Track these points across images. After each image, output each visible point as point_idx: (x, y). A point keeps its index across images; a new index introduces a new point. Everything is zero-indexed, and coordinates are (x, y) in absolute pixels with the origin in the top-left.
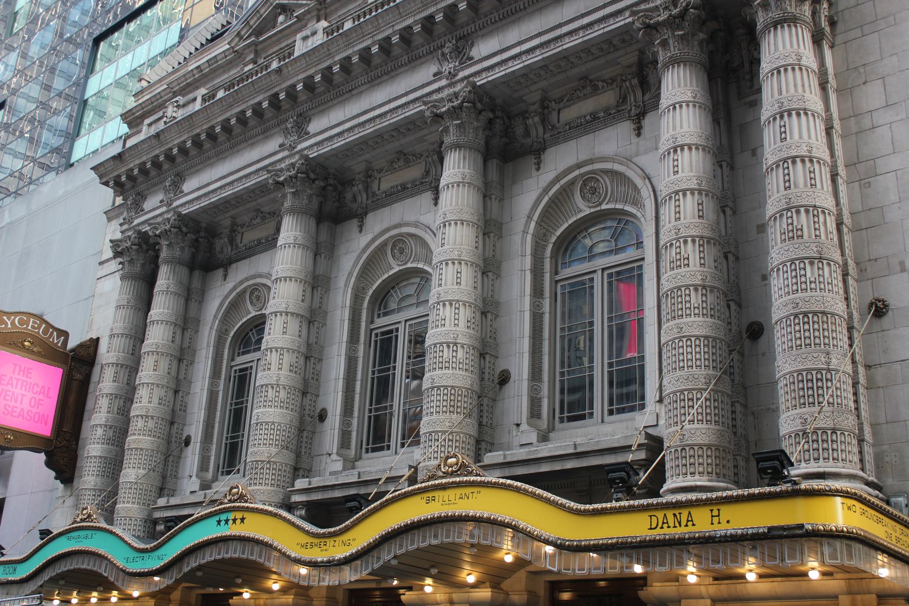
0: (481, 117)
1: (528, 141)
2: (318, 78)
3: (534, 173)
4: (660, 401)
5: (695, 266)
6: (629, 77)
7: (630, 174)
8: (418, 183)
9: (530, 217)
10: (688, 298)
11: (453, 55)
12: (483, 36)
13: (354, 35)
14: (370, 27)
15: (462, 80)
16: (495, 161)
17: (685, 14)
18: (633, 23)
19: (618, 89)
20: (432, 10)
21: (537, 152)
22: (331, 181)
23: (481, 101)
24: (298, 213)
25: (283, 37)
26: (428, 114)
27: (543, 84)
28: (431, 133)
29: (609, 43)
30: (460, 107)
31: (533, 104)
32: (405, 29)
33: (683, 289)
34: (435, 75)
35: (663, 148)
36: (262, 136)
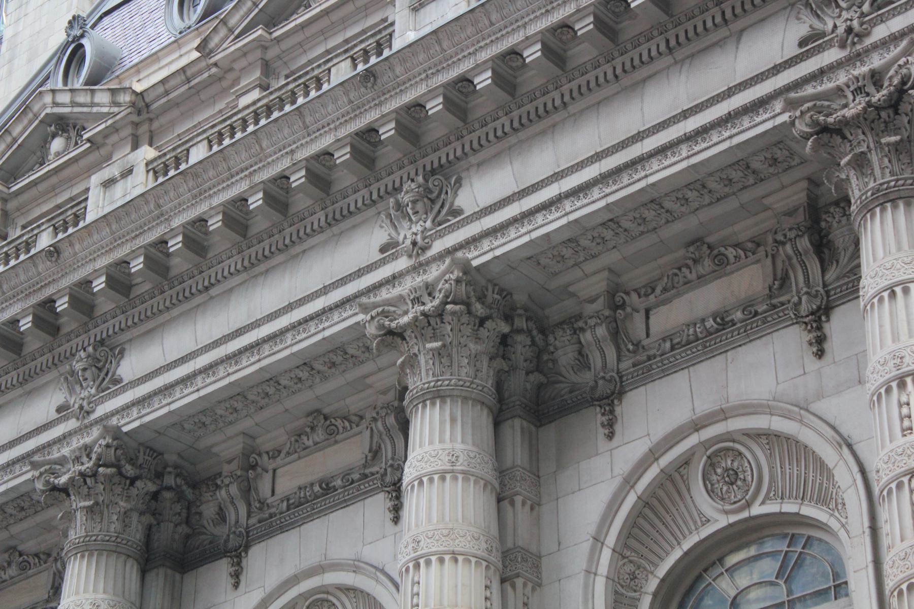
0: (483, 333)
1: (587, 377)
2: (137, 265)
3: (603, 444)
6: (791, 235)
7: (808, 437)
8: (356, 476)
9: (598, 540)
11: (419, 206)
12: (479, 165)
13: (211, 173)
14: (244, 155)
15: (441, 257)
16: (517, 422)
17: (900, 99)
18: (792, 123)
19: (769, 261)
20: (371, 117)
21: (607, 400)
22: (169, 480)
23: (481, 299)
24: (100, 552)
25: (62, 182)
26: (371, 330)
27: (611, 258)
28: (380, 370)
29: (743, 168)
30: (440, 313)
31: (592, 301)
32: (317, 157)
34: (383, 250)
35: (875, 380)
36: (19, 391)
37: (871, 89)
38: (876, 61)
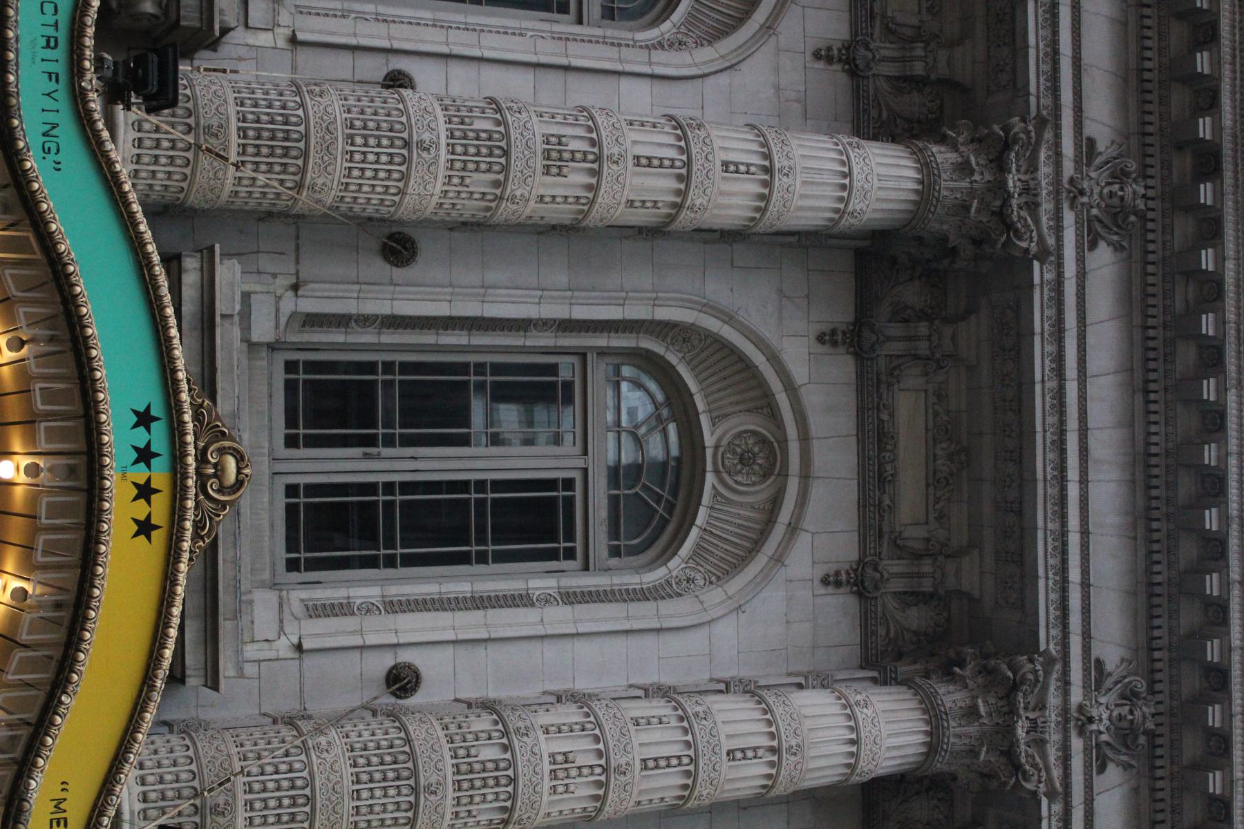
4: (293, 41)
5: (544, 185)
10: (483, 166)
17: (1004, 222)
18: (1024, 120)
33: (503, 160)
37: (1023, 199)
38: (1046, 206)
